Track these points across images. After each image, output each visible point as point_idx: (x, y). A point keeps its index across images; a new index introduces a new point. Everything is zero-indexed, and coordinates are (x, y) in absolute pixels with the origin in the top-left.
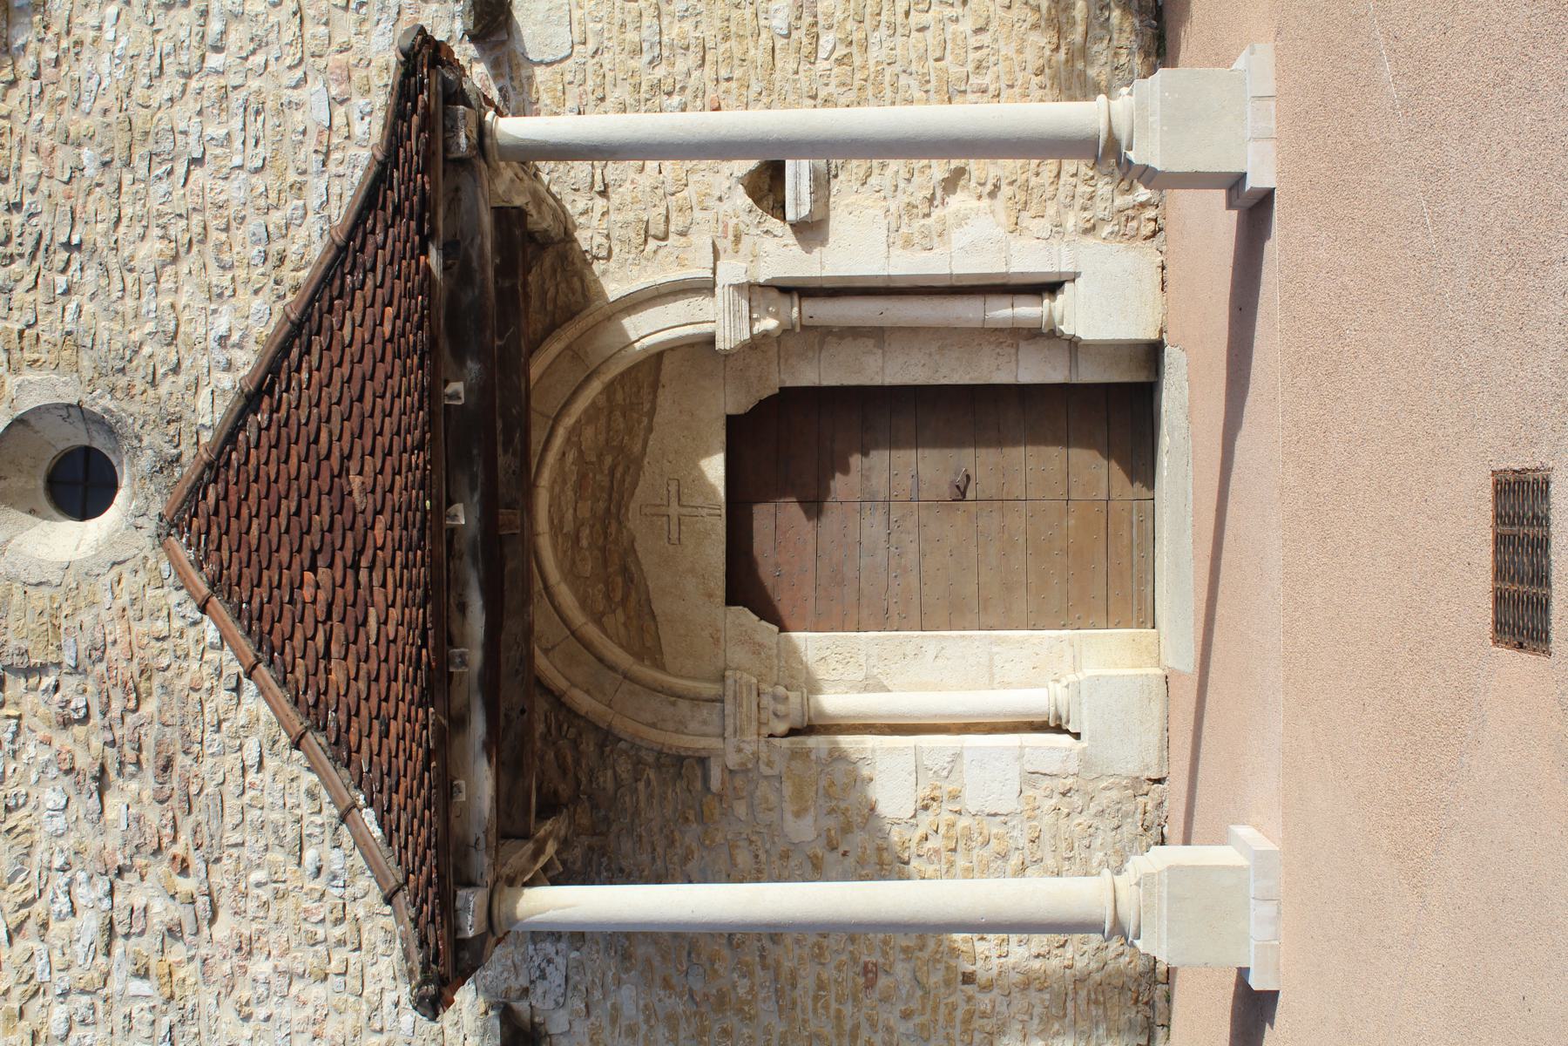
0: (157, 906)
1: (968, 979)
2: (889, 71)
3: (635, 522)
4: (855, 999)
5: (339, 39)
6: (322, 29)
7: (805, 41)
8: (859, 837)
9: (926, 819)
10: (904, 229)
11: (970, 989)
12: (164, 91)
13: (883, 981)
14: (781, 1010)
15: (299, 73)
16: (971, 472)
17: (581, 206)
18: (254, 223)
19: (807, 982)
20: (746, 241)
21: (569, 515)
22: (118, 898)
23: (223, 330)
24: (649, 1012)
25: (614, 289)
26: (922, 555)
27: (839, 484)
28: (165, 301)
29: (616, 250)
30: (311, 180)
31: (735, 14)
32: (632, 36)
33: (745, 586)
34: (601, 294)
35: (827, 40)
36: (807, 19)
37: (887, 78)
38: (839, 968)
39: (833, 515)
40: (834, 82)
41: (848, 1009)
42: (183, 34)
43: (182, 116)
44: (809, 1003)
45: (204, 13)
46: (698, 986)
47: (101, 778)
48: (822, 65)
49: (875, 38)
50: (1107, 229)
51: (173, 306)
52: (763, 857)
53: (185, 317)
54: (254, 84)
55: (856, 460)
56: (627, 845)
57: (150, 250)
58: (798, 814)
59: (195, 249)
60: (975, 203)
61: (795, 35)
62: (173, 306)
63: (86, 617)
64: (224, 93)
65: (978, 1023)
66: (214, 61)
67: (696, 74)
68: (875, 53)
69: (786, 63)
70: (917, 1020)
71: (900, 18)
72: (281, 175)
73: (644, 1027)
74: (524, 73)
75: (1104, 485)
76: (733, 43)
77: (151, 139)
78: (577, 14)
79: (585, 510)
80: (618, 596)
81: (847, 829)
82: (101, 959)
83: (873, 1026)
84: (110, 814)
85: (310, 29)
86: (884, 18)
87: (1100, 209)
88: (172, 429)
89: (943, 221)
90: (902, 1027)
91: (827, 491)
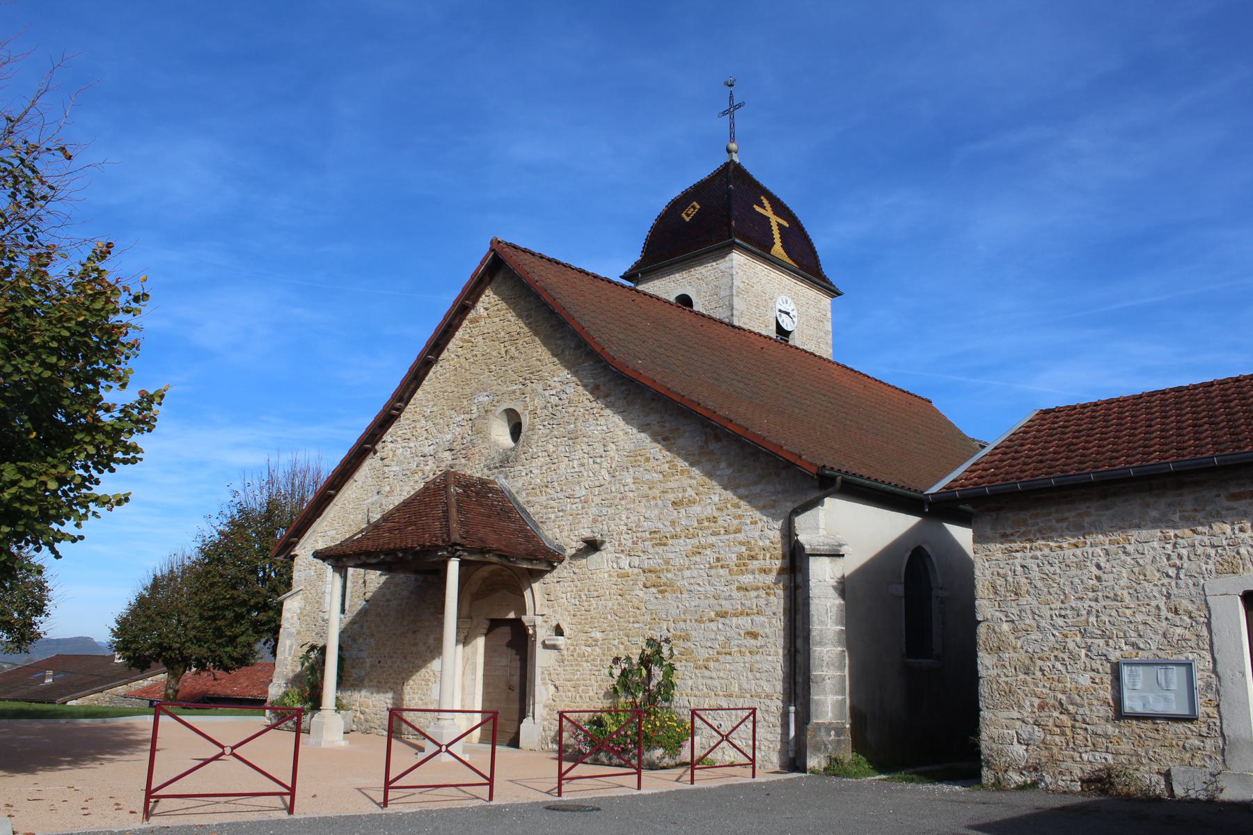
18: (555, 477)
35: (589, 649)
47: (451, 450)
64: (583, 465)
69: (584, 637)
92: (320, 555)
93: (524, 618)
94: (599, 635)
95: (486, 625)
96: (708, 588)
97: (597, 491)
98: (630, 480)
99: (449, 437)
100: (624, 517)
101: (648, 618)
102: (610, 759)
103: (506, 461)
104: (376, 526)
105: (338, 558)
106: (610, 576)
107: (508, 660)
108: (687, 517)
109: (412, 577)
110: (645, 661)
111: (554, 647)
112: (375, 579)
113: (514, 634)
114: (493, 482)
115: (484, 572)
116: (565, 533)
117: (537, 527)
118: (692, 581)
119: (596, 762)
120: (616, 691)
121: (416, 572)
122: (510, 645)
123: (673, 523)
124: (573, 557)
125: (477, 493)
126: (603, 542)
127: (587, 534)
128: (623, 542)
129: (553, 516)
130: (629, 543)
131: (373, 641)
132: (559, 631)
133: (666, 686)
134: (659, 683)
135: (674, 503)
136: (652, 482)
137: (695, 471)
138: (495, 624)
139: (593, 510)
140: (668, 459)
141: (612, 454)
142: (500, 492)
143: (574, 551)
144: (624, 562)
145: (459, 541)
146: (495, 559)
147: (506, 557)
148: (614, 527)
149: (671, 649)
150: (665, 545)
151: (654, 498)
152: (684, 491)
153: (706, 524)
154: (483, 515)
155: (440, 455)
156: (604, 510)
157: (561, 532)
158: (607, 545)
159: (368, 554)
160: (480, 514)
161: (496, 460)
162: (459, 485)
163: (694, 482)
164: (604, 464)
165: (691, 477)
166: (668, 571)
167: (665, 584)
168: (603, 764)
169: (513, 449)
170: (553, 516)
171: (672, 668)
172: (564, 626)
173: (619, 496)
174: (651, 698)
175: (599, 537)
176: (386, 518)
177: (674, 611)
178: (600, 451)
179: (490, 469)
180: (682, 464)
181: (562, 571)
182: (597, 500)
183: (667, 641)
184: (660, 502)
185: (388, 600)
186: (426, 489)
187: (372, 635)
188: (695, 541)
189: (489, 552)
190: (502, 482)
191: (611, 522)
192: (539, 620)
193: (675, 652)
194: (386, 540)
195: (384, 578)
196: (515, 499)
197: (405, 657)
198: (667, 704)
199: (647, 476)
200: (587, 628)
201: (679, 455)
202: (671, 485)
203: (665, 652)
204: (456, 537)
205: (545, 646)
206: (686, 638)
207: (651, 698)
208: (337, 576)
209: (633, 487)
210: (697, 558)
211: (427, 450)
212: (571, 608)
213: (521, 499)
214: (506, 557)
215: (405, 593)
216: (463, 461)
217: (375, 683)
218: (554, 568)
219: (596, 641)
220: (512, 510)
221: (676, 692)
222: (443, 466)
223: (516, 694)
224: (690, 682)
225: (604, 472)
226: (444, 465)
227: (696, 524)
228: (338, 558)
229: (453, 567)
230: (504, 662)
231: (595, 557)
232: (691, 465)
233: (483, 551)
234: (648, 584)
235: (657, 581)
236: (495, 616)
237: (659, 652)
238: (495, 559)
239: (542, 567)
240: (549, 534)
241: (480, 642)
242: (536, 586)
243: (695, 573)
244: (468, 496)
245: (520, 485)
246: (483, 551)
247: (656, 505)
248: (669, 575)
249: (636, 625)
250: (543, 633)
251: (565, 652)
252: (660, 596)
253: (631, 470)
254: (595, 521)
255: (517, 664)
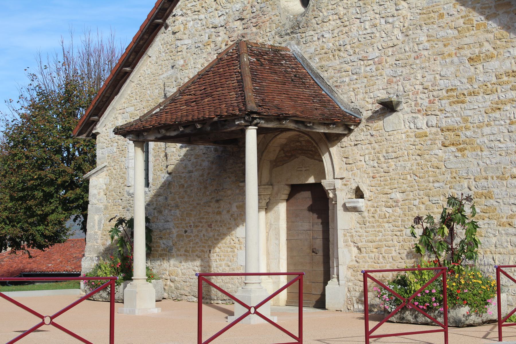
0: (220, 39)
1: (210, 251)
2: (382, 229)
3: (302, 157)
4: (206, 222)
5: (389, 60)
6: (390, 53)
7: (389, 204)
8: (233, 223)
9: (236, 240)
10: (348, 234)
11: (208, 252)
12: (376, 7)
13: (209, 229)
14: (207, 202)
15: (380, 48)
16: (318, 254)
17: (352, 138)
18: (347, 40)
19: (210, 210)
20: (344, 187)
21: (302, 139)
22: (221, 28)
23: (325, 36)
24: (204, 169)
25: (331, 149)
26: (301, 240)
27: (315, 216)
28: (331, 18)
29: (343, 149)
30: (357, 56)
31: (396, 181)
32: (390, 150)
33: (296, 189)
34: (332, 146)
35: (390, 210)
36: (394, 204)
37: (381, 229)
38: (211, 218)
39: (307, 214)
40: (380, 213)
41: (205, 220)
42: (389, 10)
43: (370, 15)
44: (205, 211)
45: (393, 16)
46: (208, 182)
47: (242, 19)
48: (384, 209)
49: (390, 225)
50: (348, 295)
51: (330, 20)
52: (230, 197)
53: (328, 24)
54: (378, 35)
55: (320, 221)
56: (231, 161)
57: (341, 10)
58: (237, 206)
59: (342, 24)
60: (354, 256)
61: (391, 200)
62: (330, 20)
63: (269, 9)
64: (375, 26)
65: (203, 253)
66: (383, 21)
67: (382, 170)
68: (386, 225)
69: (384, 198)
70: (203, 238)
71: (395, 233)
72: (357, 47)
73: (201, 168)
74: (381, 117)
75: (315, 293)
76: (390, 181)
77: (364, 6)
78: (395, 132)
79: (304, 143)
80: (287, 154)
81: (235, 220)
82: (211, 26)
83: (202, 227)
84: (236, 23)
85: (390, 50)
86: (395, 228)
87: (353, 293)
88: (305, 25)
89: (350, 246)
90: (202, 234)
91: (313, 212)
92: (120, 131)
93: (324, 183)
94: (398, 196)
95: (287, 191)
96: (510, 144)
97: (390, 51)
98: (424, 39)
99: (238, 6)
100: (419, 77)
101: (448, 176)
102: (416, 317)
103: (296, 27)
104: (173, 100)
105: (138, 133)
106: (408, 136)
107: (311, 224)
108: (483, 73)
109: (212, 147)
110: (447, 220)
111: (355, 209)
112: (176, 151)
113: (314, 198)
114: (286, 49)
115: (282, 138)
116: (360, 96)
117: (332, 91)
118: (492, 138)
119: (402, 321)
120: (418, 250)
121: (215, 142)
122: (311, 209)
123: (470, 80)
124: (370, 119)
125: (270, 61)
126: (398, 103)
127: (383, 96)
128: (420, 101)
129: (347, 79)
130: (426, 102)
131: (178, 212)
132: (359, 194)
133: (469, 244)
134: (462, 242)
135: (471, 59)
136: (447, 39)
137: (492, 25)
138: (296, 189)
139: (388, 72)
140: (463, 14)
141: (404, 12)
142: (292, 59)
143: (370, 113)
144: (422, 121)
145: (256, 109)
146: (292, 125)
147: (303, 123)
148: (407, 88)
149: (473, 207)
150: (463, 102)
151: (450, 55)
152: (481, 45)
153: (505, 79)
154: (278, 82)
155: (231, 25)
156: (399, 70)
157: (355, 95)
158: (403, 106)
159: (167, 127)
160: (274, 81)
161: (287, 26)
162: (251, 53)
163: (491, 36)
164: (397, 24)
165: (488, 31)
166: (467, 128)
167: (464, 142)
168: (409, 322)
169: (303, 15)
170: (347, 79)
171: (475, 226)
172: (364, 188)
173: (414, 55)
174: (455, 256)
175: (394, 98)
176: (182, 92)
177: (474, 169)
178: (392, 10)
179: (281, 36)
180: (477, 18)
181: (358, 133)
182: (391, 60)
183: (469, 199)
184: (456, 60)
185: (190, 172)
186: (219, 60)
187: (177, 206)
188: (494, 97)
189: (286, 118)
190: (294, 48)
191: (407, 83)
192: (338, 184)
193: (478, 210)
194: (184, 113)
195: (184, 150)
196: (308, 65)
197: (210, 226)
198: (471, 262)
199: (442, 33)
200: (387, 190)
201: (474, 8)
202: (467, 40)
203: (467, 210)
204: (252, 106)
205: (346, 209)
206: (488, 196)
207: (455, 256)
208: (139, 151)
209: (427, 45)
210: (497, 114)
211: (219, 21)
212: (370, 170)
213: (314, 64)
214: (303, 123)
215: (206, 164)
216: (254, 30)
217: (182, 252)
218: (350, 131)
219: (397, 202)
220: (306, 75)
221: (480, 250)
222: (235, 36)
223: (319, 257)
224: (494, 240)
225: (397, 32)
226: (235, 35)
227: (494, 80)
228: (138, 133)
229: (251, 135)
230: (306, 226)
231: (392, 118)
232: (488, 18)
233: (279, 118)
234: (447, 143)
235: (455, 140)
236: (296, 181)
237: (460, 210)
238: (292, 125)
239: (339, 131)
240: (344, 98)
241: (282, 208)
242: (334, 150)
243: (495, 130)
244: (262, 65)
245: (312, 50)
246: (279, 118)
247: (452, 62)
248: (468, 133)
249: (436, 185)
250: (343, 196)
251: (366, 214)
252: (459, 154)
253: (425, 28)
254: (389, 82)
255: (319, 228)
